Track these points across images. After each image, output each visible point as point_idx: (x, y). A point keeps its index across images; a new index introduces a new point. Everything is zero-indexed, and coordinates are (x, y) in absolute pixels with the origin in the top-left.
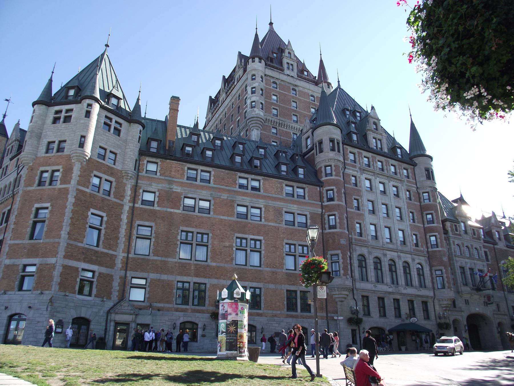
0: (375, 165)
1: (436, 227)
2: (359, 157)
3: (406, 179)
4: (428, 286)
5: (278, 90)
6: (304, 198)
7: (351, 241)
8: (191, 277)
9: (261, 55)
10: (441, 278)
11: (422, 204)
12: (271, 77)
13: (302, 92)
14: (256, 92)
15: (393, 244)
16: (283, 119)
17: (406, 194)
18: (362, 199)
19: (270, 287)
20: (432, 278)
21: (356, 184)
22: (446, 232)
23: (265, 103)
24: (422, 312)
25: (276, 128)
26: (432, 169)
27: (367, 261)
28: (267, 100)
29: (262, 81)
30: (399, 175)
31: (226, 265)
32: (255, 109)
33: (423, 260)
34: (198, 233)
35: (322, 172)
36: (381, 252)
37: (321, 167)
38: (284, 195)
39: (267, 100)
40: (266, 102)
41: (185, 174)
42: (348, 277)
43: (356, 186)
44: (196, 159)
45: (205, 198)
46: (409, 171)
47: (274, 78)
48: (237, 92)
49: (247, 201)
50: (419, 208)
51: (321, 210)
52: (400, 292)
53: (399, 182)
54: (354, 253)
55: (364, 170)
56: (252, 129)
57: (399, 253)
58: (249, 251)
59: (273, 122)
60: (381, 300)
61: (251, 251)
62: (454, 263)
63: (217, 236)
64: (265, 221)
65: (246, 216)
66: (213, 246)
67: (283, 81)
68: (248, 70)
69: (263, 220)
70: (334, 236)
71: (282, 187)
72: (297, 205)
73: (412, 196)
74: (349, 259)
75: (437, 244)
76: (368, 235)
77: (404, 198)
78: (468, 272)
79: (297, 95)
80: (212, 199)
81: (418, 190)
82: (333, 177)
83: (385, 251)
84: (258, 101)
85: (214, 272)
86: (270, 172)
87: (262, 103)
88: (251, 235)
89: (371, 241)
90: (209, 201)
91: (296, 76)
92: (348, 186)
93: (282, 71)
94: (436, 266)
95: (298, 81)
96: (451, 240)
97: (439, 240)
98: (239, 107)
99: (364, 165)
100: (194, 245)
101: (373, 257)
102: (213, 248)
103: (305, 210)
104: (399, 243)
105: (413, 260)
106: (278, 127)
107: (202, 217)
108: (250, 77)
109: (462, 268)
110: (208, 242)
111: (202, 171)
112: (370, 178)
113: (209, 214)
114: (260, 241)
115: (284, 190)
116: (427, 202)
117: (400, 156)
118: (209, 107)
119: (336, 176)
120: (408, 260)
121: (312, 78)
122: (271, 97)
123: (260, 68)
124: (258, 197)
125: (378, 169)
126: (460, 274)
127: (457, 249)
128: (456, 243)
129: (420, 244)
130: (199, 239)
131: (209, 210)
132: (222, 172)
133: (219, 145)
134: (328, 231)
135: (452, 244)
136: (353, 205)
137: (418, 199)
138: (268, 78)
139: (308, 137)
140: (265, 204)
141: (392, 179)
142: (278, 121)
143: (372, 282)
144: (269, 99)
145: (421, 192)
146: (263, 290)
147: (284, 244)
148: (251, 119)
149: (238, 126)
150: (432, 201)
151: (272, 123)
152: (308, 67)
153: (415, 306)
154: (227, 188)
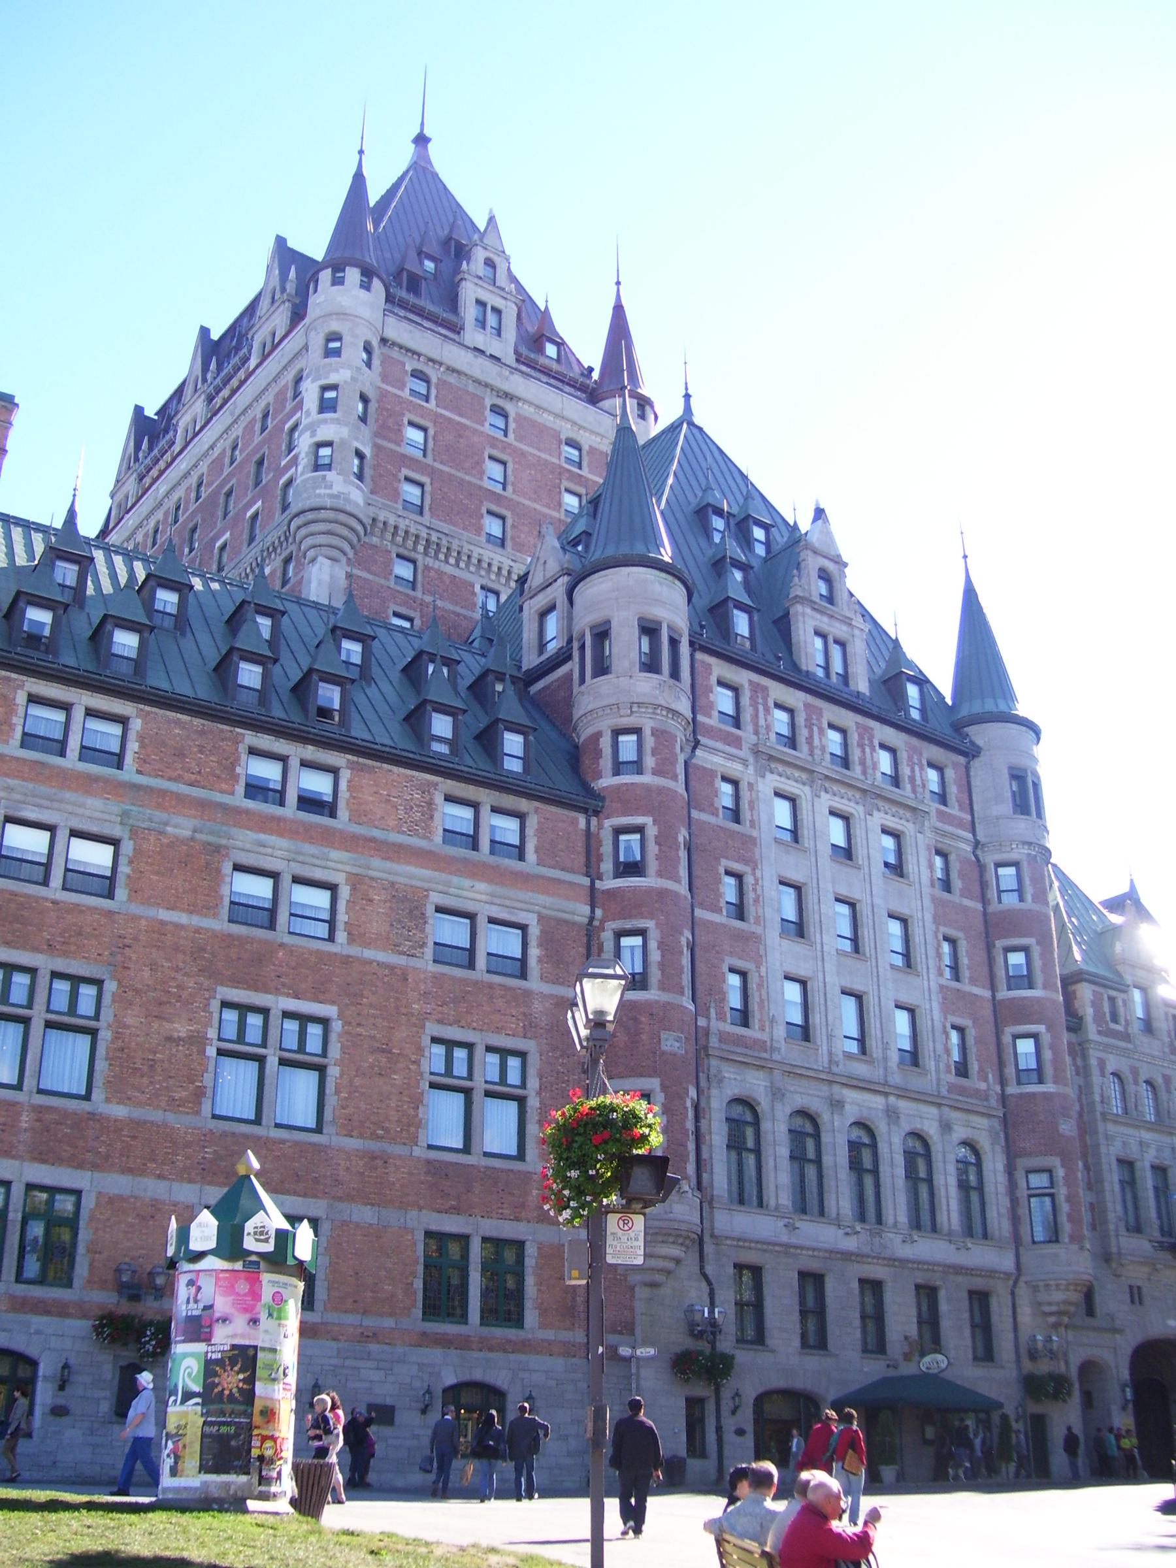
0: (816, 742)
1: (1038, 1000)
2: (754, 704)
3: (934, 806)
4: (997, 1232)
5: (432, 405)
6: (521, 857)
7: (702, 1042)
8: (15, 1163)
9: (372, 259)
10: (1047, 1200)
11: (990, 909)
12: (408, 350)
13: (533, 424)
14: (339, 408)
15: (871, 1062)
16: (446, 527)
17: (931, 866)
18: (758, 873)
19: (355, 1218)
20: (1014, 1202)
21: (735, 814)
22: (1075, 1024)
23: (376, 456)
24: (967, 1332)
26: (1036, 774)
27: (766, 1126)
28: (385, 443)
29: (369, 364)
30: (908, 787)
31: (170, 1118)
32: (331, 476)
33: (982, 1130)
34: (55, 975)
35: (598, 753)
36: (824, 1090)
37: (598, 735)
38: (438, 837)
39: (385, 443)
40: (377, 448)
41: (17, 721)
42: (686, 1188)
43: (737, 819)
44: (68, 659)
45: (94, 829)
46: (950, 773)
47: (419, 355)
48: (256, 399)
50: (978, 922)
51: (587, 910)
52: (887, 1254)
53: (908, 815)
54: (714, 1092)
55: (771, 758)
56: (310, 554)
57: (892, 1099)
58: (272, 1062)
60: (811, 1281)
61: (283, 1062)
62: (1098, 1145)
63: (137, 991)
64: (351, 939)
65: (269, 916)
66: (117, 1036)
67: (454, 371)
68: (313, 311)
69: (341, 936)
70: (635, 1019)
71: (430, 803)
72: (490, 881)
73: (954, 875)
74: (691, 1114)
75: (1039, 1070)
76: (773, 1021)
77: (925, 879)
78: (1147, 1181)
79: (511, 435)
80: (126, 836)
81: (979, 852)
82: (646, 779)
83: (836, 1089)
84: (343, 442)
85: (118, 1145)
86: (383, 738)
87: (360, 455)
88: (288, 995)
89: (783, 1046)
90: (114, 842)
91: (510, 359)
92: (704, 817)
93: (453, 331)
94: (1030, 1154)
95: (517, 378)
96: (1094, 1055)
97: (1047, 1055)
98: (260, 463)
99: (773, 737)
100: (37, 1026)
101: (789, 1111)
102: (120, 1043)
103: (519, 905)
104: (894, 1057)
105: (946, 1127)
106: (420, 558)
107: (77, 909)
108: (317, 342)
109: (1127, 1164)
110: (97, 1017)
111: (90, 713)
112: (797, 791)
113: (110, 895)
114: (324, 1022)
115: (437, 815)
116: (1010, 900)
117: (915, 715)
119: (656, 772)
120: (925, 1128)
121: (575, 373)
122: (399, 431)
123: (366, 312)
124: (328, 838)
125: (828, 757)
126: (1117, 1187)
127: (1113, 1091)
128: (1110, 1068)
129: (974, 1067)
130: (61, 1002)
131: (112, 879)
132: (178, 723)
133: (172, 609)
135: (1095, 1071)
136: (719, 895)
137: (976, 889)
138: (395, 353)
139: (552, 608)
140: (355, 870)
141: (881, 804)
142: (424, 533)
143: (778, 1212)
144: (390, 441)
145: (989, 859)
147: (426, 1040)
148: (310, 516)
149: (252, 539)
150: (1029, 898)
151: (399, 539)
152: (563, 326)
153: (944, 1307)
154: (196, 792)
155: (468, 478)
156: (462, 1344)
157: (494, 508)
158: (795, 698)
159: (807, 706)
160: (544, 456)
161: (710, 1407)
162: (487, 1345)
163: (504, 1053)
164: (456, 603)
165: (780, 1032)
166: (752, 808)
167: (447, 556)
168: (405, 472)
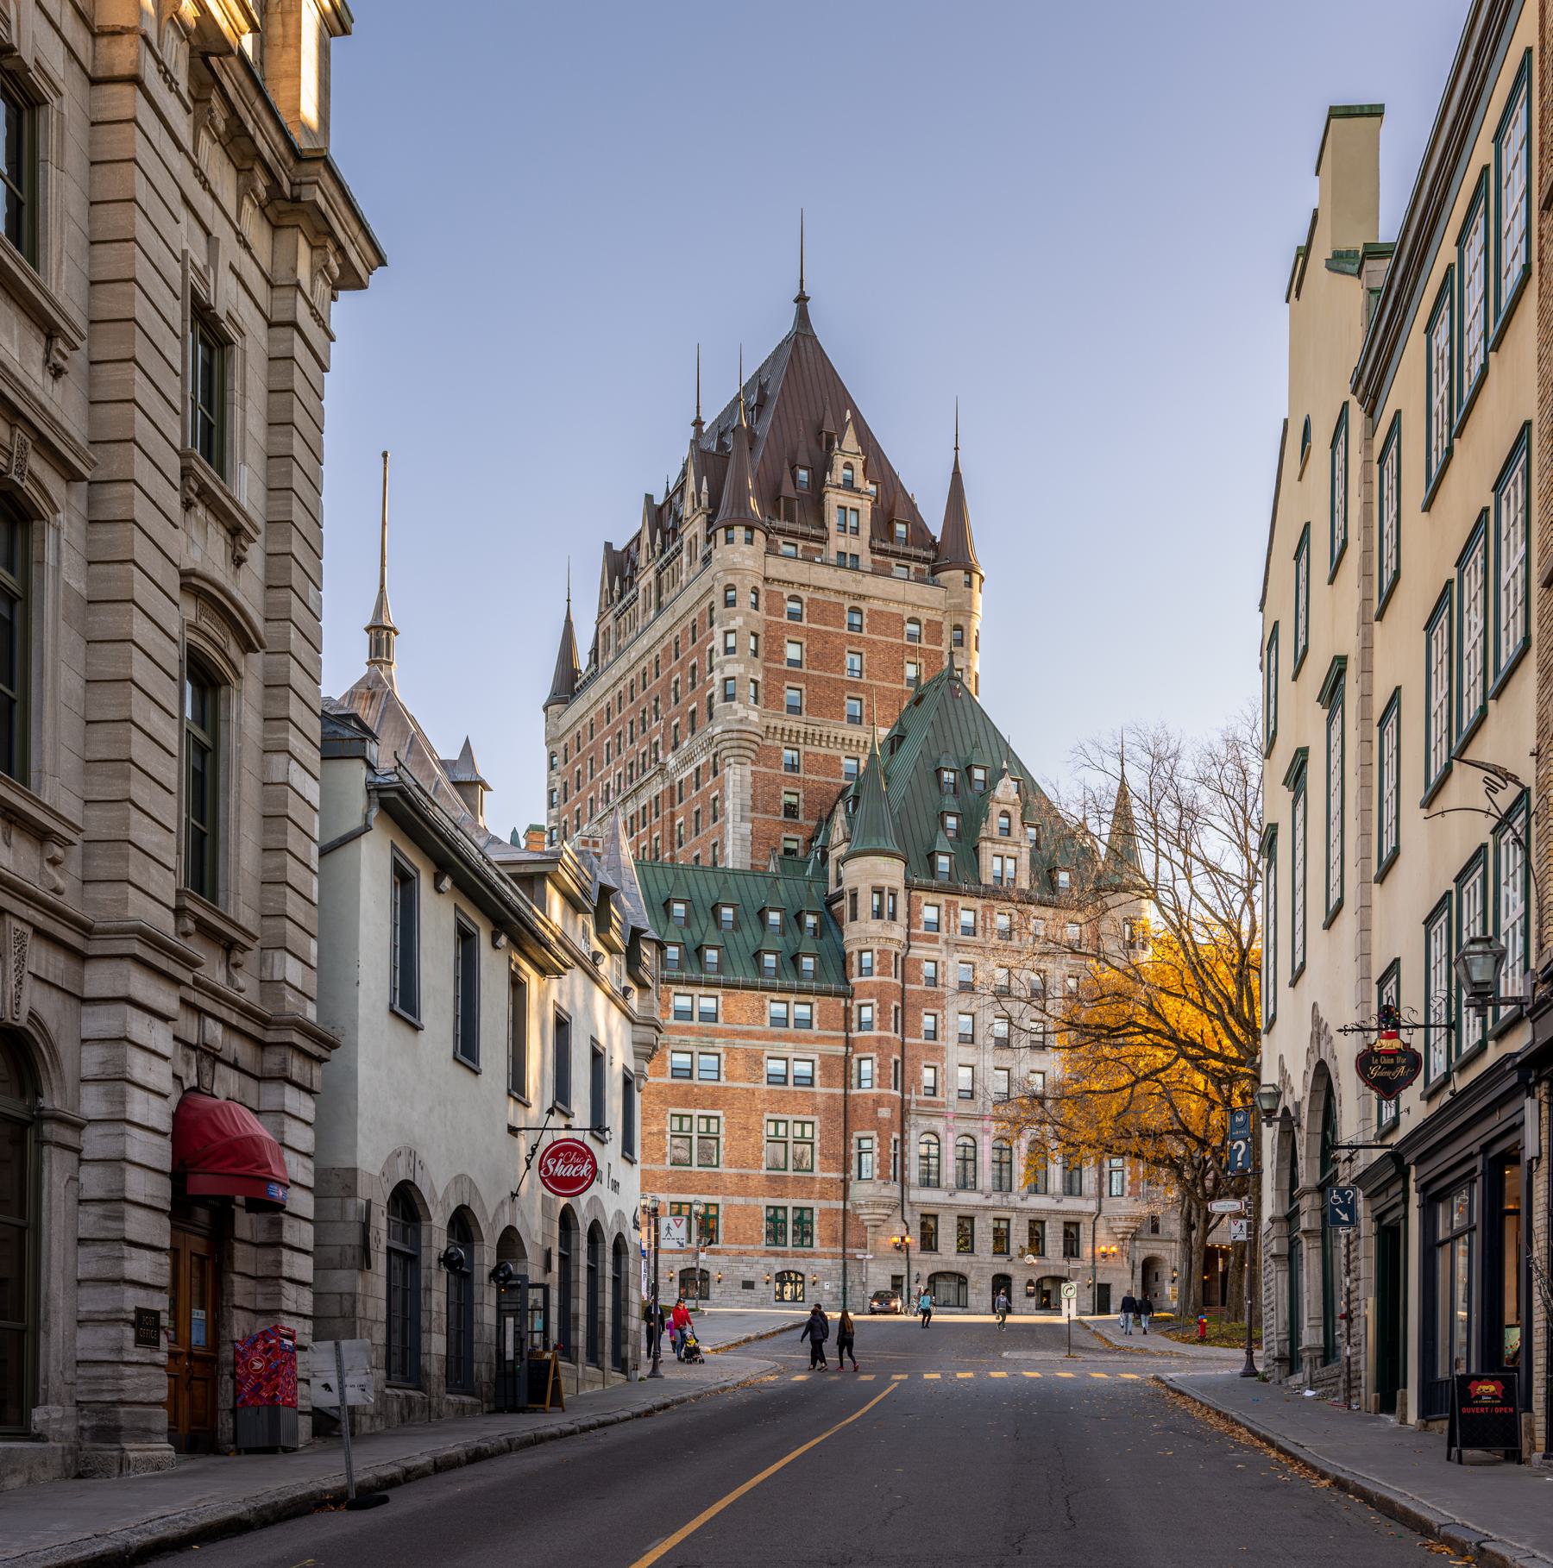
2: (948, 914)
5: (804, 623)
13: (880, 613)
16: (817, 720)
23: (765, 677)
25: (798, 750)
27: (942, 1145)
32: (735, 705)
36: (979, 1125)
37: (852, 953)
38: (767, 1024)
40: (767, 670)
49: (692, 1042)
51: (844, 1049)
59: (787, 732)
64: (728, 1078)
69: (723, 1078)
71: (763, 1007)
79: (865, 629)
82: (875, 978)
91: (866, 560)
99: (959, 931)
106: (801, 747)
114: (718, 1118)
115: (767, 1012)
118: (607, 586)
119: (879, 975)
134: (854, 1091)
142: (802, 728)
144: (775, 662)
146: (721, 1208)
147: (765, 1121)
151: (786, 738)
155: (833, 676)
156: (784, 1255)
157: (853, 694)
158: (978, 904)
159: (984, 907)
160: (890, 640)
161: (905, 1279)
162: (796, 1255)
163: (803, 1123)
164: (828, 775)
165: (954, 1096)
166: (943, 977)
167: (820, 741)
168: (788, 683)
